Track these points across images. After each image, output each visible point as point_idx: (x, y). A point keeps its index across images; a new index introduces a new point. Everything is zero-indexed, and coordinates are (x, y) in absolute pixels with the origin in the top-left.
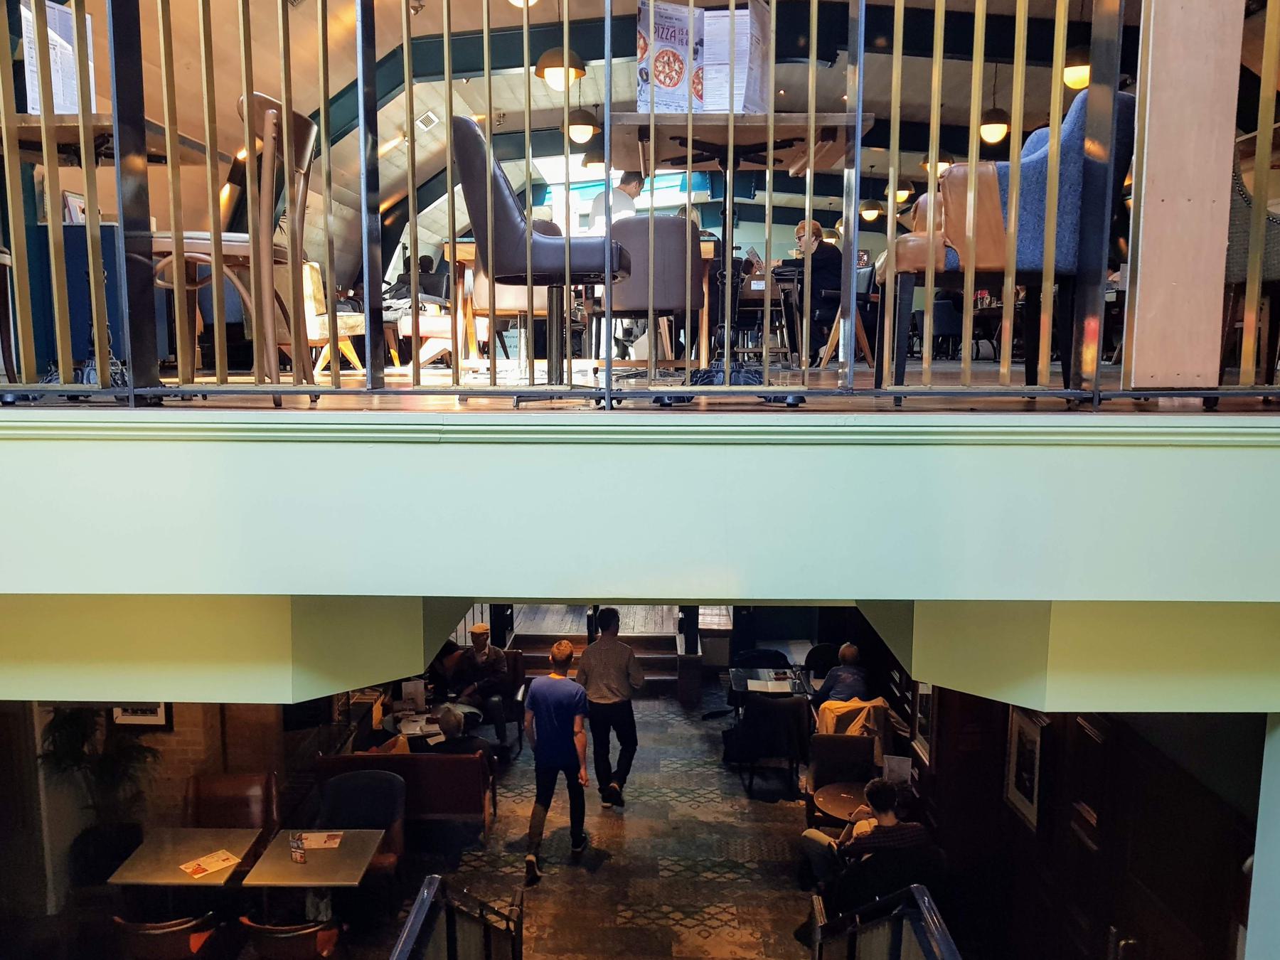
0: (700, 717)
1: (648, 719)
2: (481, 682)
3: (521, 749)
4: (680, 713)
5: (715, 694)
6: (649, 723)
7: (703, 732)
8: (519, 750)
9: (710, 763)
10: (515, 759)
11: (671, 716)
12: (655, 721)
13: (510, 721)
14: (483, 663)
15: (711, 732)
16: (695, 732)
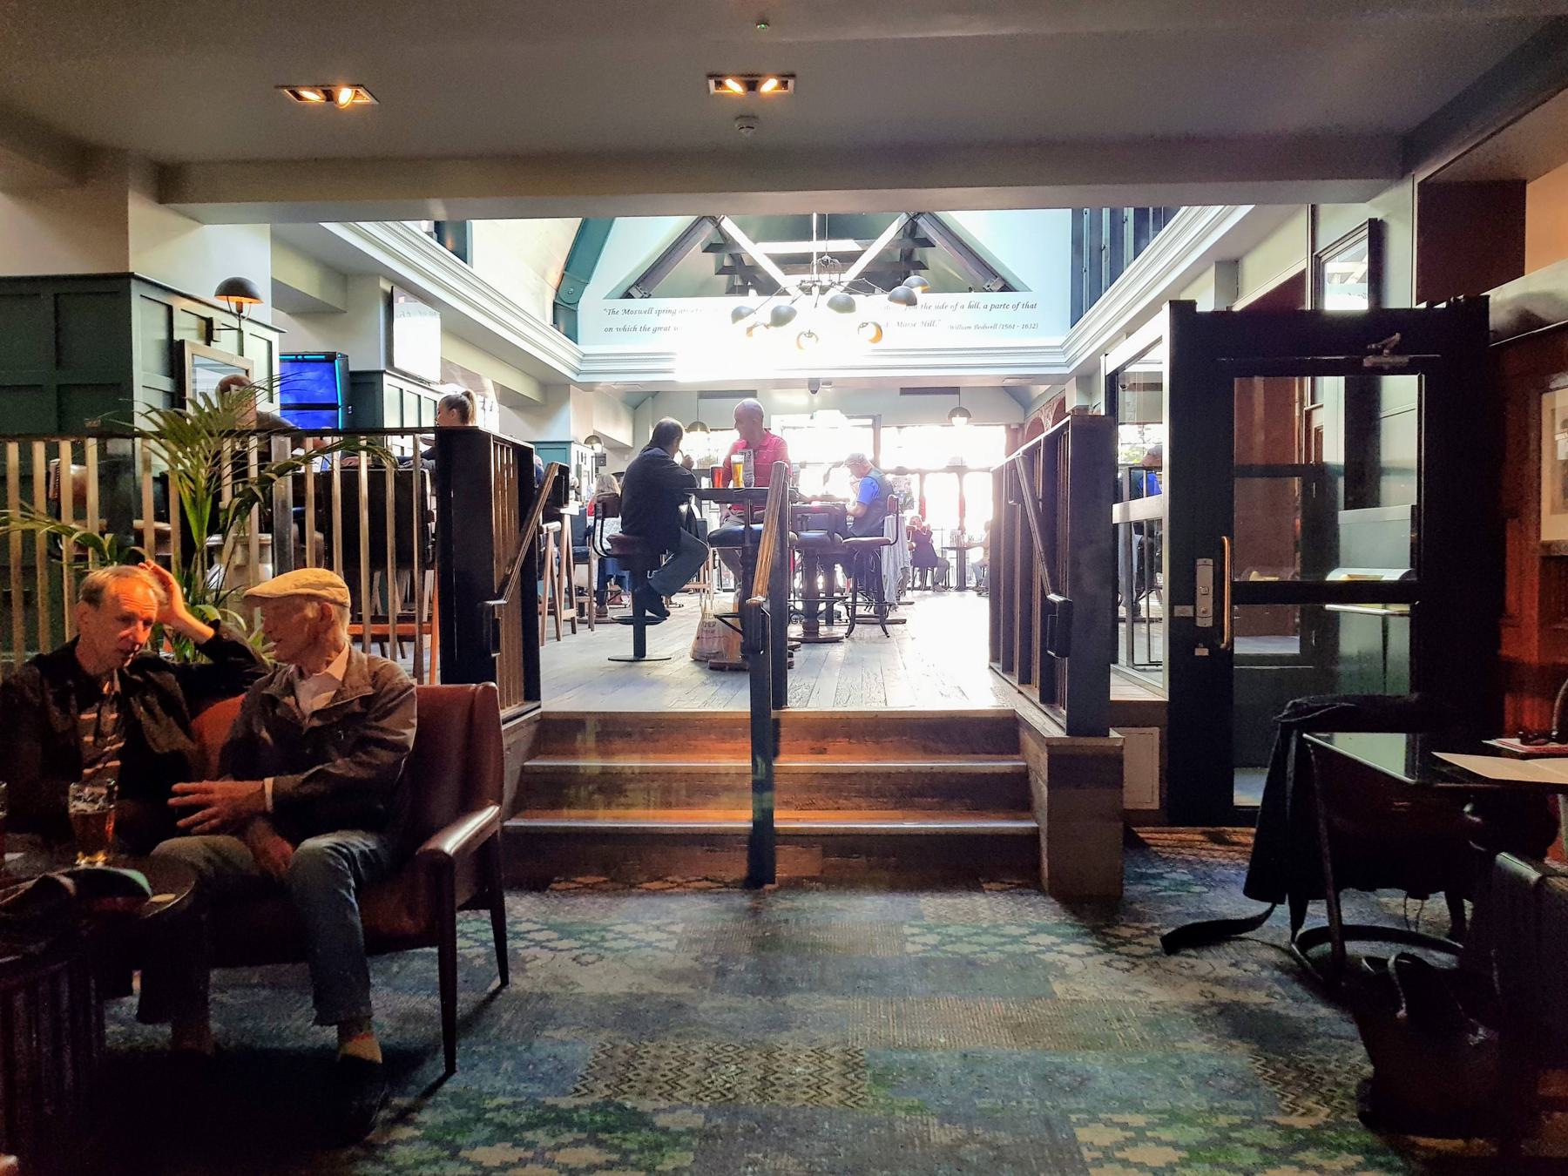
0: (1157, 942)
1: (965, 949)
2: (290, 781)
3: (451, 1069)
4: (1070, 930)
5: (1161, 877)
6: (972, 963)
7: (1191, 994)
8: (441, 1072)
9: (1312, 1139)
10: (403, 1117)
11: (1045, 939)
12: (994, 956)
13: (389, 943)
14: (315, 714)
15: (1224, 995)
16: (1159, 995)
